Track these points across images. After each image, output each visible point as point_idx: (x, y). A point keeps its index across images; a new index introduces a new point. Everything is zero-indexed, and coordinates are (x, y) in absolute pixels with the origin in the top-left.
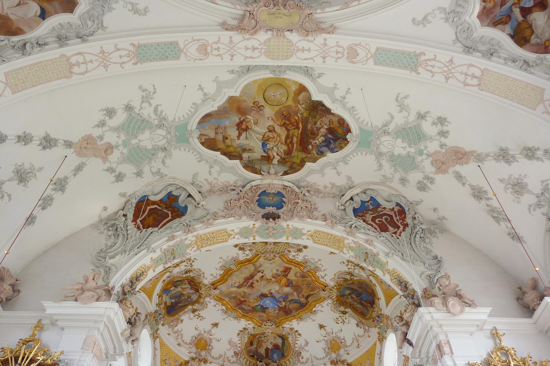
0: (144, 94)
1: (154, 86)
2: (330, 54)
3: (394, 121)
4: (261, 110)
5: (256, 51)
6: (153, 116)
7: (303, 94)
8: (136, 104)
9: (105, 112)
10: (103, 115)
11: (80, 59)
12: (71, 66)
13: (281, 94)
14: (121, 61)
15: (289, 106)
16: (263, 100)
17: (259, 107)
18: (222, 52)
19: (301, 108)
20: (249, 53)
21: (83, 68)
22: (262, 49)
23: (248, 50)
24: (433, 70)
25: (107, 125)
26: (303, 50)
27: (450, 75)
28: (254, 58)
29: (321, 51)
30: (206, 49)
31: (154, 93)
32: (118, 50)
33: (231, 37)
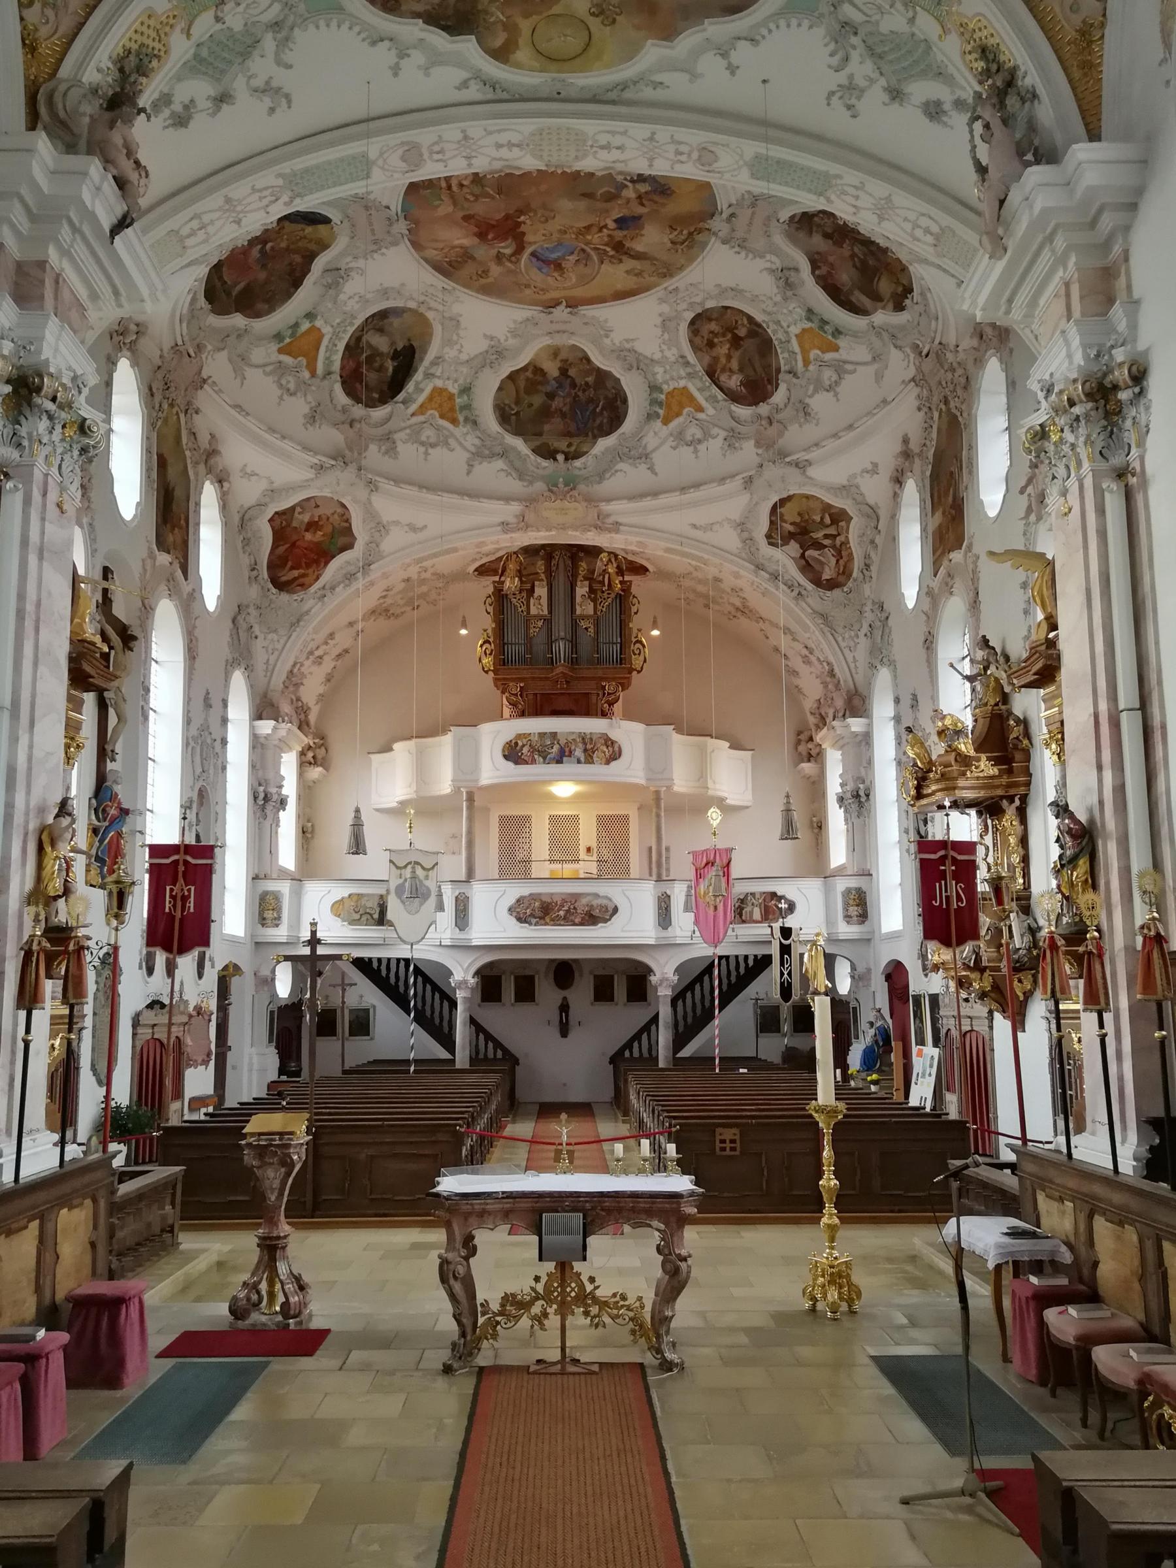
0: (853, 101)
1: (829, 104)
2: (457, 146)
3: (270, 56)
4: (597, 5)
5: (604, 143)
6: (855, 56)
7: (498, 42)
8: (876, 94)
9: (945, 119)
10: (950, 117)
11: (919, 233)
12: (937, 238)
13: (549, 40)
14: (860, 193)
15: (527, 15)
16: (593, 29)
17: (602, 13)
18: (672, 148)
19: (497, 15)
20: (617, 140)
21: (924, 222)
22: (592, 146)
23: (619, 144)
24: (258, 194)
25: (956, 97)
26: (511, 145)
27: (227, 207)
28: (608, 132)
29: (474, 147)
30: (700, 156)
31: (832, 93)
32: (855, 206)
33: (651, 166)
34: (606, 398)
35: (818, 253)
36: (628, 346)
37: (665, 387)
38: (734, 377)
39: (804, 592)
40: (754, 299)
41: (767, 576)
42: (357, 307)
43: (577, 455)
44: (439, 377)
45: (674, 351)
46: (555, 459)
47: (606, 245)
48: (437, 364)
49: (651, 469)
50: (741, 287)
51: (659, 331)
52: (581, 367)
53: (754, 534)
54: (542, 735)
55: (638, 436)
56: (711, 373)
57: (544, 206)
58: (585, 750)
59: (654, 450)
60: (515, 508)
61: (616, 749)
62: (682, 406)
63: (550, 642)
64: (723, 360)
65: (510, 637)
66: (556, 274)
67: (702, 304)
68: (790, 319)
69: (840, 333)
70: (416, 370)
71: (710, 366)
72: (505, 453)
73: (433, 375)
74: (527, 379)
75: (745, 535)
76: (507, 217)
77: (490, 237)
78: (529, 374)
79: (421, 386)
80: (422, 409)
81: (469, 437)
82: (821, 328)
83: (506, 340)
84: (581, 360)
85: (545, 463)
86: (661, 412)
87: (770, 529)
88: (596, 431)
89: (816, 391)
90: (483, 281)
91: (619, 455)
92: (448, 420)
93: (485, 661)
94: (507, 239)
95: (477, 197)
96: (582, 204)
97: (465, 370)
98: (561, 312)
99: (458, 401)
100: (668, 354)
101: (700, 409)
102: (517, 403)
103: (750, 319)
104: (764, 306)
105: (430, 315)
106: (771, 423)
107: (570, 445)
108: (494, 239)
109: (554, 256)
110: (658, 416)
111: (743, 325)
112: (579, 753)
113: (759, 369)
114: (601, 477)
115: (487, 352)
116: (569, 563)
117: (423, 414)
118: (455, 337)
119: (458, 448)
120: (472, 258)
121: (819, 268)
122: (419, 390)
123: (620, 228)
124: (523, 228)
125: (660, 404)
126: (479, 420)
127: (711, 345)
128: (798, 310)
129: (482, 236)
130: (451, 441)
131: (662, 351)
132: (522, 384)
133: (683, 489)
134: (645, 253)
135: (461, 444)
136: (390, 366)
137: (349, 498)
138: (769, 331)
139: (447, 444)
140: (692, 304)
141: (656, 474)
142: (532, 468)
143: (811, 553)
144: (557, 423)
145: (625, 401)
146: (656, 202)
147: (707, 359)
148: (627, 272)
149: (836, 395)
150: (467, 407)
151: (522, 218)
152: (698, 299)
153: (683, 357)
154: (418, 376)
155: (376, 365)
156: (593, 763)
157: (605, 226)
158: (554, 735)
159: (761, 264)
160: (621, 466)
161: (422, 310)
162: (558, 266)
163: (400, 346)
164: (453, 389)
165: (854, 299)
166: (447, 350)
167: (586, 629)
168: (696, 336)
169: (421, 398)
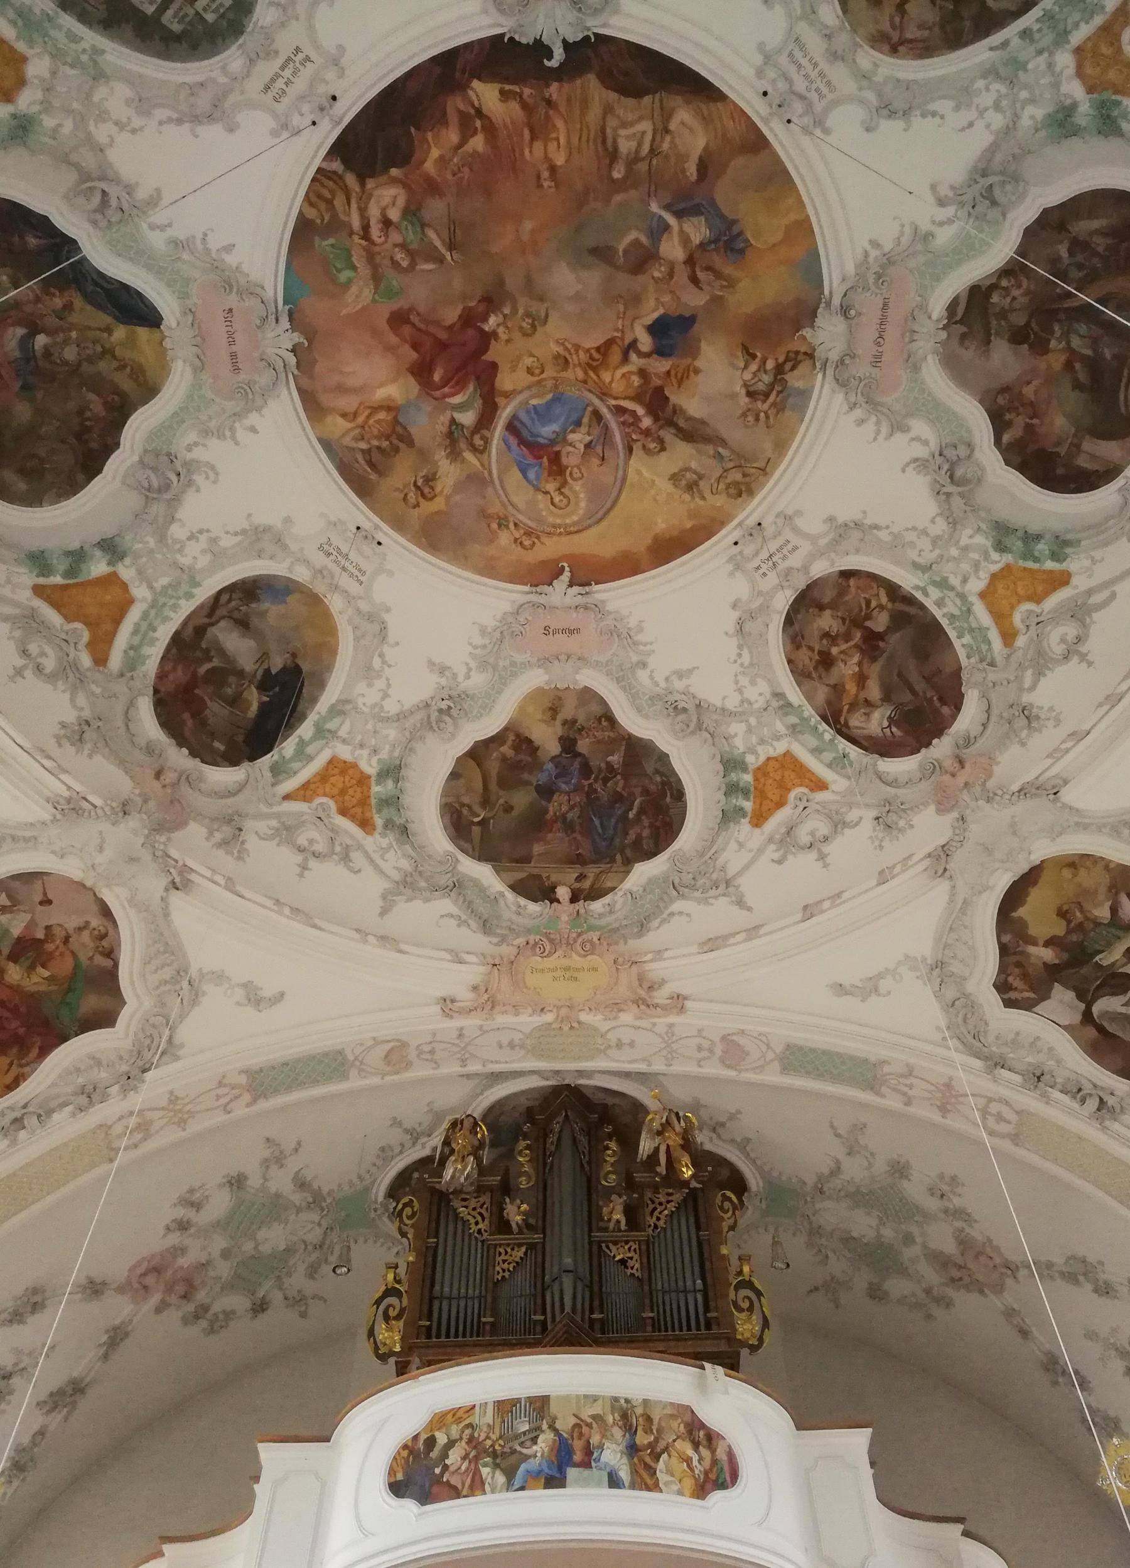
34: (646, 792)
35: (1005, 389)
36: (679, 685)
37: (750, 759)
38: (876, 715)
39: (1111, 1101)
40: (897, 546)
41: (1018, 1079)
42: (203, 561)
43: (595, 894)
44: (344, 741)
45: (763, 687)
46: (554, 900)
47: (637, 398)
48: (342, 713)
49: (740, 903)
50: (868, 521)
51: (734, 642)
52: (599, 735)
53: (970, 987)
54: (506, 1408)
55: (708, 850)
56: (834, 717)
57: (529, 285)
58: (633, 1449)
59: (739, 874)
60: (474, 972)
61: (721, 1454)
62: (784, 788)
63: (541, 1286)
64: (851, 688)
65: (446, 1285)
66: (551, 486)
67: (806, 568)
68: (965, 567)
69: (1067, 543)
70: (303, 718)
71: (829, 703)
72: (457, 887)
73: (333, 733)
74: (504, 759)
75: (950, 993)
76: (468, 319)
77: (437, 377)
78: (506, 749)
79: (310, 750)
80: (305, 792)
81: (390, 855)
82: (1028, 555)
83: (468, 677)
84: (599, 720)
85: (533, 907)
86: (748, 805)
87: (1003, 969)
88: (628, 852)
89: (1039, 674)
90: (428, 507)
91: (675, 887)
92: (353, 818)
93: (383, 1333)
94: (461, 386)
95: (412, 254)
96: (594, 278)
97: (391, 733)
98: (560, 593)
99: (376, 789)
100: (751, 693)
101: (821, 785)
102: (485, 802)
103: (893, 590)
104: (913, 555)
105: (335, 604)
106: (961, 763)
107: (581, 878)
108: (445, 383)
109: (547, 431)
110: (741, 809)
111: (881, 607)
112: (612, 1455)
113: (920, 686)
114: (642, 927)
115: (432, 698)
116: (583, 1140)
117: (306, 799)
118: (377, 663)
119: (369, 870)
120: (410, 443)
121: (1009, 424)
122: (302, 755)
123: (660, 351)
124: (495, 352)
125: (746, 793)
126: (412, 827)
127: (826, 661)
128: (980, 539)
129: (421, 371)
130: (356, 856)
131: (740, 691)
132: (493, 766)
133: (809, 911)
134: (703, 422)
135: (372, 861)
136: (254, 699)
137: (123, 892)
138: (928, 603)
139: (346, 858)
140: (789, 571)
141: (749, 909)
142: (507, 914)
143: (1106, 1005)
144: (557, 841)
145: (679, 795)
146: (718, 275)
147: (822, 693)
148: (674, 478)
149: (1083, 657)
150: (392, 802)
151: (493, 321)
152: (795, 561)
153: (779, 695)
154: (306, 730)
155: (229, 691)
156: (655, 1487)
157: (633, 344)
158: (540, 1405)
159: (903, 448)
160: (678, 905)
161: (319, 588)
162: (557, 468)
163: (277, 663)
164: (369, 766)
165: (1083, 462)
166: (361, 687)
167: (623, 1262)
168: (798, 647)
169: (307, 772)
